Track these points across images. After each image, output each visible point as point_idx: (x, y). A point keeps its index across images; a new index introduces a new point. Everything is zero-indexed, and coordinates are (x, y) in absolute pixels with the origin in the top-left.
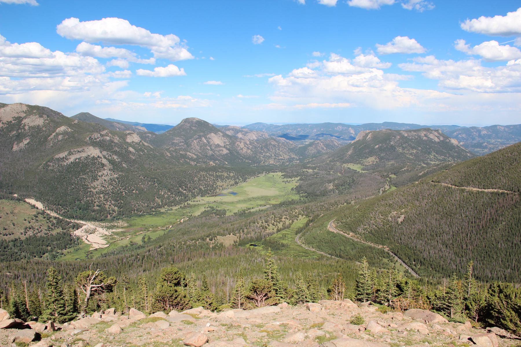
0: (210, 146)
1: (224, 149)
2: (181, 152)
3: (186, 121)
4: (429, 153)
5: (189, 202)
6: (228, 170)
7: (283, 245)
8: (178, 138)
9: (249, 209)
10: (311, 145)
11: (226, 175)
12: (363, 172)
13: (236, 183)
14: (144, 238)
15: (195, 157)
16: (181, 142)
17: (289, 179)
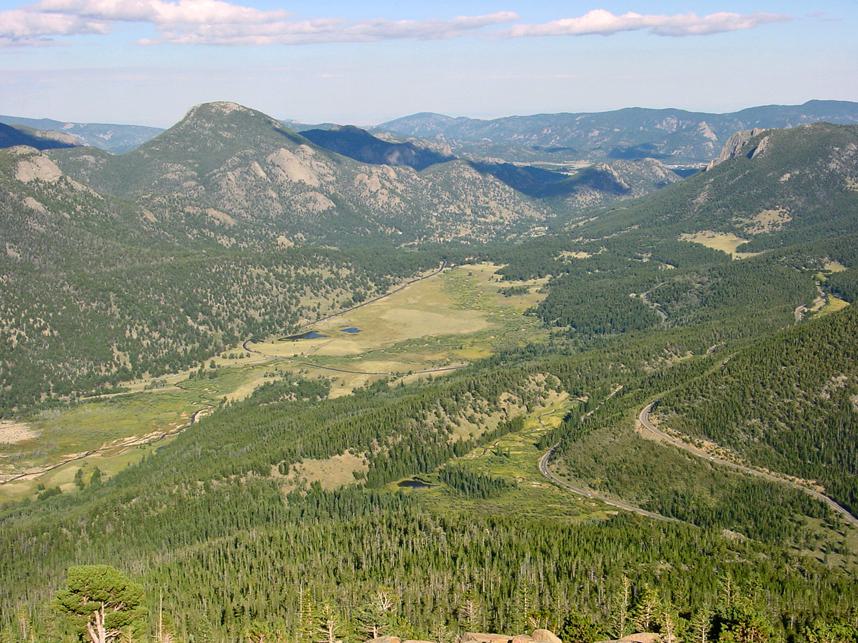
0: (279, 189)
1: (320, 197)
2: (188, 209)
3: (203, 112)
5: (219, 361)
6: (335, 259)
7: (500, 483)
8: (177, 167)
9: (399, 375)
11: (326, 274)
12: (744, 256)
13: (359, 298)
14: (80, 473)
15: (232, 222)
16: (186, 180)
17: (519, 284)
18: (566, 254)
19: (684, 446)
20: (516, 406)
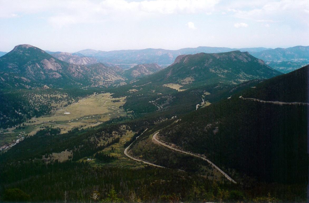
1: (57, 74)
2: (15, 77)
3: (19, 48)
4: (239, 72)
5: (25, 123)
8: (12, 64)
9: (82, 126)
10: (135, 68)
12: (181, 90)
13: (70, 103)
16: (14, 68)
17: (117, 99)
18: (131, 90)
19: (166, 145)
20: (117, 135)
